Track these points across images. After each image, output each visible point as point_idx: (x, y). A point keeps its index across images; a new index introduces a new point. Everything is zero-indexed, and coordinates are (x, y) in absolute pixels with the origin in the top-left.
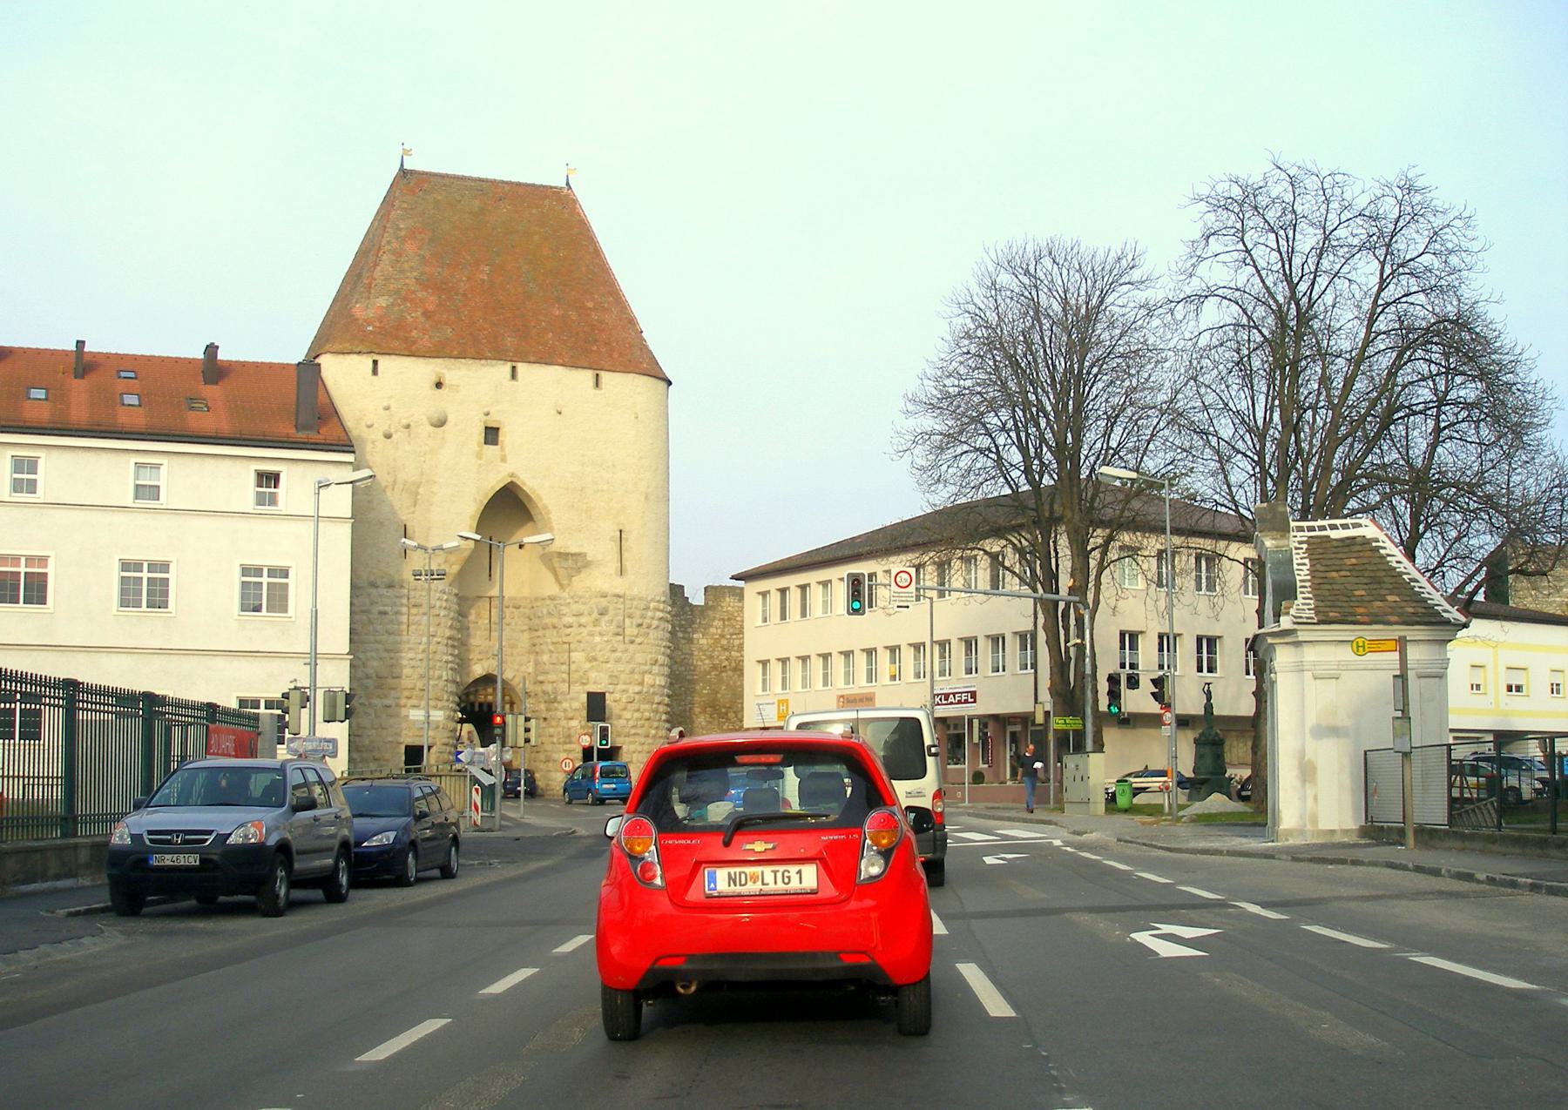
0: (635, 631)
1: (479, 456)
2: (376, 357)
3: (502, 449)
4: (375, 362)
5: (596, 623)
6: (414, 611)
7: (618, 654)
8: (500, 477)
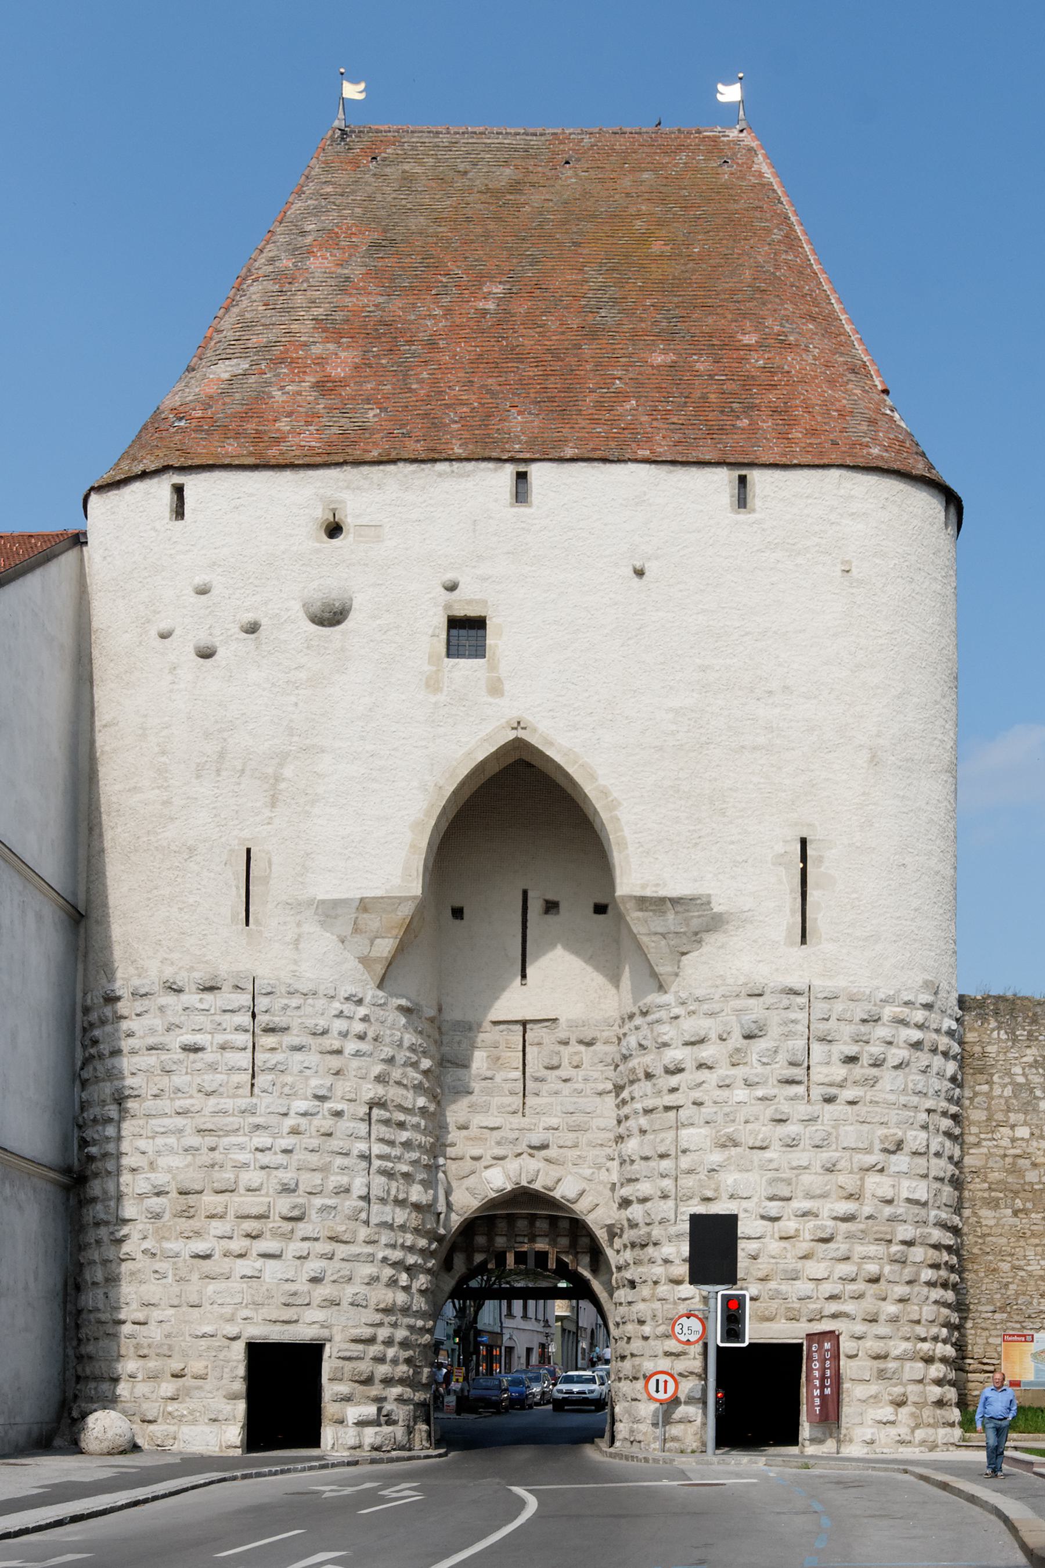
1: (433, 684)
6: (269, 1040)
7: (791, 1129)
8: (488, 728)
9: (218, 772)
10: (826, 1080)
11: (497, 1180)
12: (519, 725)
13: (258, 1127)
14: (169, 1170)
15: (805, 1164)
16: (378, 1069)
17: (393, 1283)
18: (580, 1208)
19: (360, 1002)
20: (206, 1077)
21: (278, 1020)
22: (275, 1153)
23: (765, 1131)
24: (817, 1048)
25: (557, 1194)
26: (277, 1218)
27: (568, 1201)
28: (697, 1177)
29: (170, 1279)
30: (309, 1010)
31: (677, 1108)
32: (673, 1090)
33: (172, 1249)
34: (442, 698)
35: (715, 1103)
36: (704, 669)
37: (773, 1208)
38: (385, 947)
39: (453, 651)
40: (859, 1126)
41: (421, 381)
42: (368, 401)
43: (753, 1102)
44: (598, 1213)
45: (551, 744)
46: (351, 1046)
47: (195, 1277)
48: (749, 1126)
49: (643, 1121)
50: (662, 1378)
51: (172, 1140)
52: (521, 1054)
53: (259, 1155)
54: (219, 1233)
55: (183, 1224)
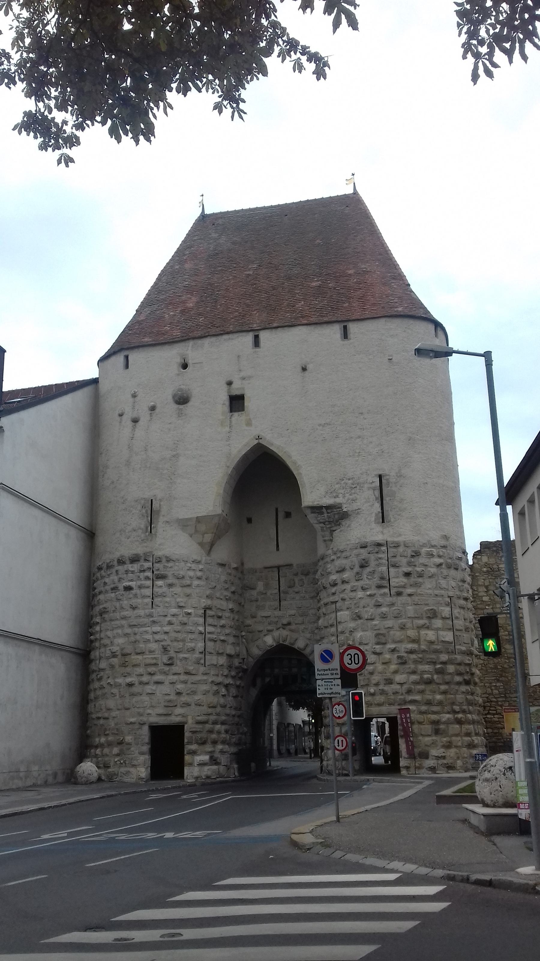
0: (403, 580)
2: (126, 353)
4: (127, 357)
5: (358, 577)
6: (160, 583)
7: (384, 609)
10: (397, 585)
11: (269, 641)
12: (259, 438)
13: (154, 622)
15: (391, 626)
16: (208, 592)
17: (216, 693)
19: (199, 562)
20: (133, 601)
22: (162, 634)
24: (392, 570)
25: (296, 647)
26: (162, 665)
27: (301, 649)
28: (345, 635)
29: (118, 697)
30: (176, 568)
32: (334, 594)
33: (118, 682)
35: (351, 599)
37: (378, 648)
38: (208, 538)
40: (414, 607)
43: (366, 597)
46: (196, 582)
47: (127, 695)
48: (365, 609)
51: (119, 631)
52: (278, 582)
53: (155, 636)
54: (138, 673)
55: (123, 670)
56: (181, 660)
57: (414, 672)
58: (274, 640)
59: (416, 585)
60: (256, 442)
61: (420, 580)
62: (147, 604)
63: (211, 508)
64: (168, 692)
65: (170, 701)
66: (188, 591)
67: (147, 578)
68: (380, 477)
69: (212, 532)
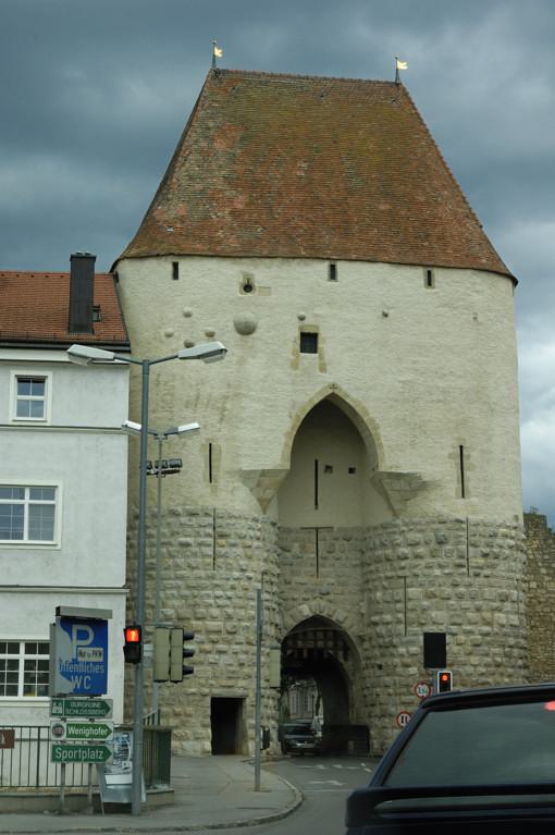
3: (321, 358)
6: (222, 541)
7: (462, 589)
9: (196, 405)
11: (306, 611)
13: (217, 586)
14: (173, 607)
18: (345, 626)
21: (226, 531)
23: (448, 590)
25: (334, 619)
31: (405, 577)
34: (298, 372)
36: (415, 362)
39: (303, 350)
41: (279, 214)
42: (256, 223)
44: (352, 627)
45: (348, 396)
49: (385, 583)
50: (405, 715)
56: (243, 629)
57: (487, 655)
58: (311, 610)
59: (493, 567)
60: (330, 391)
61: (496, 561)
62: (209, 565)
63: (279, 462)
64: (231, 662)
65: (234, 672)
66: (249, 552)
67: (208, 535)
68: (461, 447)
69: (277, 489)
